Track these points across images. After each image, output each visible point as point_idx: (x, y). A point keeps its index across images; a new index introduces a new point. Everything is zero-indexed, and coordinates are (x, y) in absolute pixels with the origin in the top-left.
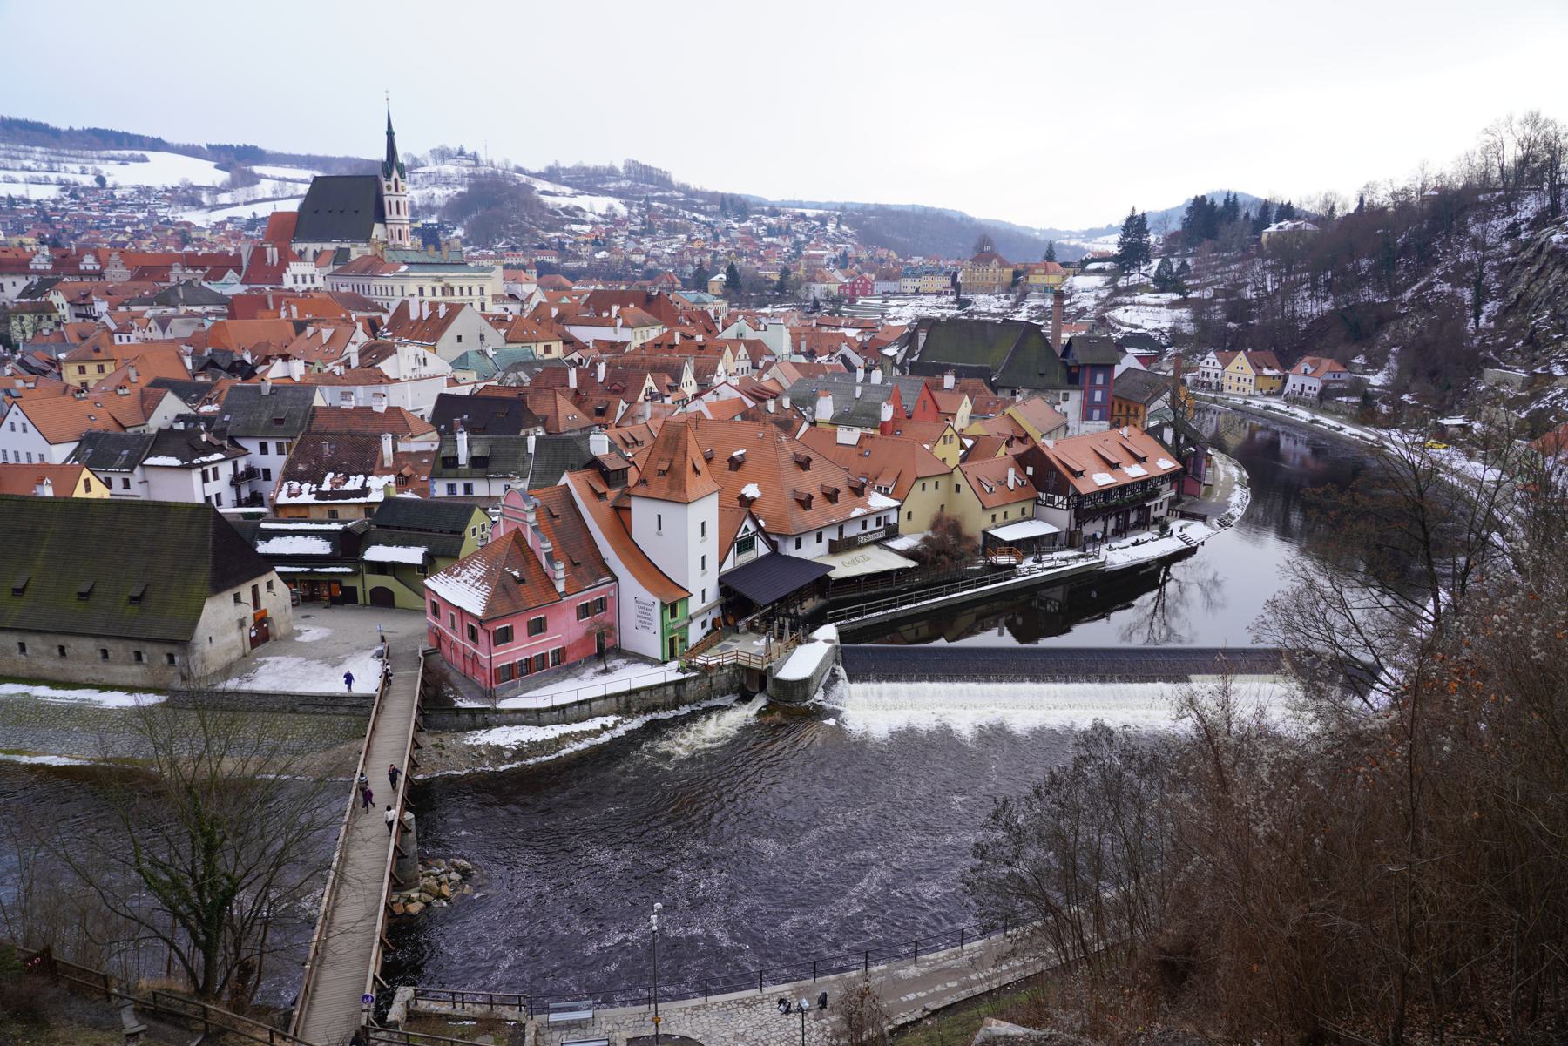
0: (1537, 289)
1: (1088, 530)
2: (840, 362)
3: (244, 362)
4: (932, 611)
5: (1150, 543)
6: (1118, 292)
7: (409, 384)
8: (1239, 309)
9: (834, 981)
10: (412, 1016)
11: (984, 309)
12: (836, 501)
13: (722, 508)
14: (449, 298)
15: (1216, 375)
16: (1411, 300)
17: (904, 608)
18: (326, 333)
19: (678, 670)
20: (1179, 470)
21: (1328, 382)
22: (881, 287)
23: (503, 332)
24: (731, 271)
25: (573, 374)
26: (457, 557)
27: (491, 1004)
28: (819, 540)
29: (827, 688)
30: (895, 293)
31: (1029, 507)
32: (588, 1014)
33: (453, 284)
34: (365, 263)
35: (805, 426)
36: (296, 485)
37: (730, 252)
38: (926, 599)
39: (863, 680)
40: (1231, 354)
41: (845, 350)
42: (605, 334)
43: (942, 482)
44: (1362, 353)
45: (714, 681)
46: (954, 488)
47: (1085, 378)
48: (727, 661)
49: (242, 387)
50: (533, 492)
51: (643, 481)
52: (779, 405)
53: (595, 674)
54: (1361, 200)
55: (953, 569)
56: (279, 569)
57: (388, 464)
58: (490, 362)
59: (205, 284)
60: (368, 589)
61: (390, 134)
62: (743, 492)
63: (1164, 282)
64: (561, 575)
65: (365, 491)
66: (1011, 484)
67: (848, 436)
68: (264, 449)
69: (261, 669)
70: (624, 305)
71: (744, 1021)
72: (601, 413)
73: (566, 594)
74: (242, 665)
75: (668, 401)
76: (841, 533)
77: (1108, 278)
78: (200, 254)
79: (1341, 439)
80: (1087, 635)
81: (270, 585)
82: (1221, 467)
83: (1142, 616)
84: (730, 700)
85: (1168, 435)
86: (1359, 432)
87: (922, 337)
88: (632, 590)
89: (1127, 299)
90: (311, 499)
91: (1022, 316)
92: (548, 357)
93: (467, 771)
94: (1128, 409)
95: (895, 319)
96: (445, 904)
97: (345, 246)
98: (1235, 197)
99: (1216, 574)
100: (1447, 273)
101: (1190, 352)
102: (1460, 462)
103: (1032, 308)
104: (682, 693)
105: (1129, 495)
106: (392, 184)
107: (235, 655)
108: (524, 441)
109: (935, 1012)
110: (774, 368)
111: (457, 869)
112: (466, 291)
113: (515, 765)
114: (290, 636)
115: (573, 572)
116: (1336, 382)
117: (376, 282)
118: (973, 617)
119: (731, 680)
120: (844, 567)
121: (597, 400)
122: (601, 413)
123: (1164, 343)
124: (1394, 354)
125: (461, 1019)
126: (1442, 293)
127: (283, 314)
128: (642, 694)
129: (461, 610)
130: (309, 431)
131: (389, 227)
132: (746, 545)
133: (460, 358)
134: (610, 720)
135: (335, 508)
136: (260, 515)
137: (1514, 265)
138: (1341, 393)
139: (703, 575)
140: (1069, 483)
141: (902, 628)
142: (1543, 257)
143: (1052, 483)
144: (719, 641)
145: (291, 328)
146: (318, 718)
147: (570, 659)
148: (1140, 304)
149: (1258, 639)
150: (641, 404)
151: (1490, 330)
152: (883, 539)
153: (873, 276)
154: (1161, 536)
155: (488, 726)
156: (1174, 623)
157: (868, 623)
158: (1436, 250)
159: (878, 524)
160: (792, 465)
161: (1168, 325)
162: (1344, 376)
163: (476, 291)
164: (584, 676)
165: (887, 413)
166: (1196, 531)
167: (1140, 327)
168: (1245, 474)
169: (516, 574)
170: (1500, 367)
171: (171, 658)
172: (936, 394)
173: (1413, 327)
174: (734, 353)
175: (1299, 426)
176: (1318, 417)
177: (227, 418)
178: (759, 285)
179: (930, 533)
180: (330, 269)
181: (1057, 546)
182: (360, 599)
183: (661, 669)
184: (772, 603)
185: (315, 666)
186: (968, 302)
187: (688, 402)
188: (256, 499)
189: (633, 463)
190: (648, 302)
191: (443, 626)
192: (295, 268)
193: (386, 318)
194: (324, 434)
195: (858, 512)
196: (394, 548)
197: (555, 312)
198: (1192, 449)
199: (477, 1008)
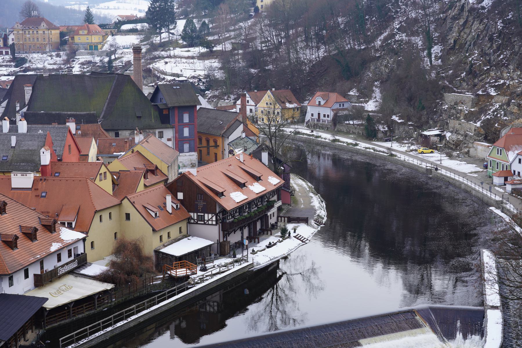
0: (465, 36)
1: (234, 238)
4: (140, 324)
5: (278, 244)
6: (154, 47)
11: (40, 66)
12: (36, 239)
15: (251, 110)
16: (382, 46)
17: (119, 324)
28: (27, 276)
31: (184, 225)
38: (133, 314)
40: (259, 94)
44: (355, 87)
46: (124, 216)
47: (174, 117)
66: (169, 209)
76: (42, 268)
77: (142, 36)
85: (265, 156)
91: (76, 70)
94: (208, 141)
101: (225, 94)
102: (447, 162)
103: (83, 64)
123: (202, 88)
124: (376, 87)
126: (402, 41)
137: (445, 19)
138: (347, 118)
140: (216, 202)
142: (465, 14)
143: (201, 204)
148: (175, 57)
151: (440, 66)
156: (288, 307)
157: (94, 343)
159: (70, 256)
161: (202, 73)
162: (346, 105)
165: (46, 158)
167: (182, 76)
168: (309, 184)
170: (455, 92)
173: (386, 66)
175: (324, 145)
176: (337, 138)
179: (114, 258)
181: (213, 256)
186: (23, 61)
195: (55, 247)
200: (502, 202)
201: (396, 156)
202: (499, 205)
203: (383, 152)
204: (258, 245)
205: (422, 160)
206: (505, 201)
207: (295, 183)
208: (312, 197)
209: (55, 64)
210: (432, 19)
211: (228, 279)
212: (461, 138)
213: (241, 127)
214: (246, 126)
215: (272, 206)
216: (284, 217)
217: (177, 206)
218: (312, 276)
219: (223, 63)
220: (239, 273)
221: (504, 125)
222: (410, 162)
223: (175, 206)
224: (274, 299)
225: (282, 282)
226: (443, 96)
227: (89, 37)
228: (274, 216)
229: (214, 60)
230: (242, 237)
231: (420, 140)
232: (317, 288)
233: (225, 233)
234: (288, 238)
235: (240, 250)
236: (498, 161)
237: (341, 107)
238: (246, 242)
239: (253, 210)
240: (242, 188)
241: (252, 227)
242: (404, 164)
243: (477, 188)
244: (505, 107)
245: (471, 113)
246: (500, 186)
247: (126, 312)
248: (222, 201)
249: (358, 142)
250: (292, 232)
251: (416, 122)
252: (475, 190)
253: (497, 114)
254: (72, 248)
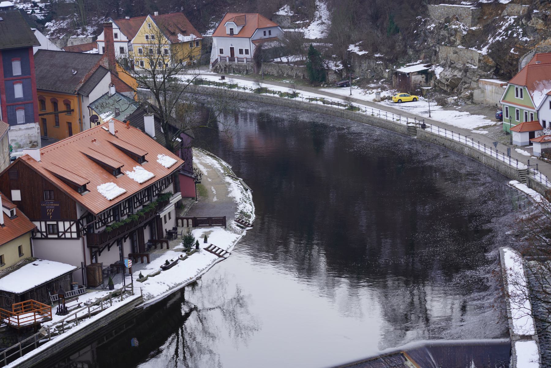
5: (181, 262)
15: (122, 49)
21: (262, 41)
31: (25, 243)
79: (299, 107)
85: (149, 122)
86: (318, 96)
94: (55, 104)
99: (239, 291)
116: (271, 40)
123: (40, 17)
138: (277, 52)
143: (51, 206)
162: (275, 33)
168: (224, 163)
175: (244, 98)
176: (264, 85)
181: (76, 289)
200: (528, 172)
201: (359, 109)
202: (523, 176)
203: (338, 104)
204: (148, 266)
205: (400, 113)
206: (532, 170)
207: (201, 163)
208: (229, 184)
211: (103, 324)
212: (458, 74)
213: (108, 78)
214: (115, 75)
215: (167, 203)
216: (187, 219)
217: (12, 212)
218: (238, 310)
220: (120, 314)
221: (523, 50)
222: (382, 117)
223: (8, 213)
224: (180, 351)
225: (191, 323)
226: (427, 9)
228: (170, 218)
230: (122, 256)
231: (395, 81)
232: (246, 328)
233: (94, 250)
234: (195, 251)
235: (119, 276)
236: (518, 107)
237: (267, 36)
238: (128, 263)
239: (135, 211)
240: (115, 176)
241: (136, 237)
242: (373, 122)
243: (488, 152)
244: (524, 21)
245: (471, 34)
246: (523, 147)
248: (85, 199)
249: (297, 91)
250: (201, 241)
251: (386, 54)
252: (484, 155)
253: (512, 34)
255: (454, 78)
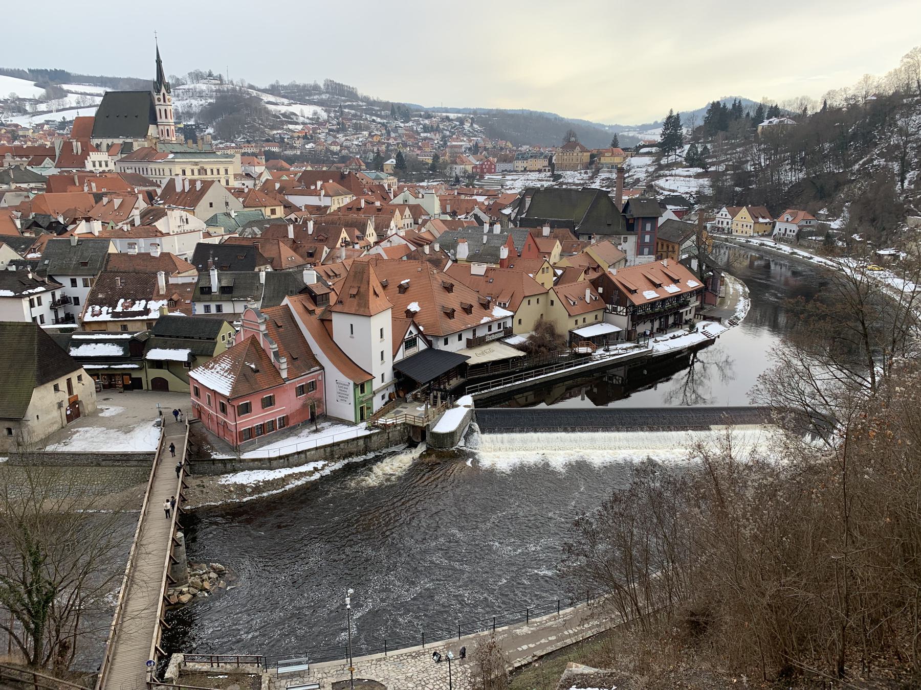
1: (641, 328)
2: (473, 219)
3: (59, 222)
4: (536, 385)
6: (661, 167)
7: (176, 236)
8: (742, 178)
9: (472, 639)
10: (182, 674)
11: (570, 181)
13: (394, 319)
14: (203, 177)
16: (858, 170)
17: (517, 383)
18: (117, 202)
19: (366, 429)
20: (702, 288)
22: (501, 167)
23: (241, 200)
24: (399, 157)
25: (291, 228)
26: (212, 356)
27: (238, 663)
28: (460, 339)
29: (466, 438)
30: (510, 171)
31: (600, 314)
32: (305, 667)
33: (206, 166)
34: (145, 152)
35: (450, 263)
36: (97, 308)
37: (398, 144)
38: (532, 377)
39: (490, 432)
40: (737, 209)
41: (477, 210)
42: (313, 201)
43: (541, 298)
44: (826, 207)
45: (390, 435)
48: (399, 422)
49: (57, 240)
50: (263, 310)
51: (340, 302)
52: (432, 249)
53: (309, 433)
54: (825, 103)
55: (549, 357)
56: (86, 367)
57: (162, 292)
58: (233, 220)
59: (29, 168)
60: (150, 378)
61: (159, 62)
62: (409, 308)
63: (692, 161)
64: (284, 366)
65: (146, 311)
66: (588, 300)
67: (478, 269)
68: (74, 283)
69: (75, 437)
70: (325, 180)
71: (412, 668)
72: (311, 255)
73: (288, 379)
74: (62, 434)
75: (357, 247)
76: (474, 334)
78: (25, 146)
79: (811, 265)
80: (641, 399)
81: (80, 378)
82: (731, 285)
83: (678, 386)
84: (402, 446)
85: (694, 264)
86: (824, 260)
87: (528, 201)
88: (334, 375)
89: (667, 172)
90: (105, 317)
91: (596, 185)
92: (273, 217)
93: (221, 502)
94: (668, 247)
95: (510, 189)
96: (206, 595)
97: (129, 140)
98: (740, 102)
100: (882, 152)
101: (710, 208)
103: (603, 180)
104: (369, 444)
105: (668, 305)
106: (161, 97)
107: (55, 427)
108: (257, 275)
109: (541, 657)
110: (429, 223)
111: (214, 570)
112: (215, 172)
113: (254, 497)
114: (96, 413)
115: (293, 364)
117: (152, 166)
118: (564, 388)
119: (402, 434)
120: (477, 357)
121: (308, 247)
122: (311, 255)
123: (692, 202)
124: (847, 207)
125: (217, 674)
126: (879, 165)
127: (86, 189)
128: (342, 446)
129: (215, 392)
130: (106, 270)
131: (161, 127)
132: (411, 343)
133: (212, 218)
134: (320, 464)
135: (125, 323)
136: (72, 329)
138: (811, 234)
139: (382, 363)
140: (627, 297)
141: (516, 397)
143: (615, 298)
144: (394, 408)
145: (93, 201)
146: (116, 469)
147: (292, 423)
148: (676, 175)
149: (754, 401)
150: (339, 249)
151: (911, 190)
152: (502, 338)
153: (496, 160)
154: (690, 332)
155: (235, 471)
156: (700, 391)
157: (493, 394)
158: (875, 137)
159: (499, 327)
160: (441, 288)
161: (695, 190)
162: (813, 223)
163: (222, 172)
164: (301, 434)
165: (504, 253)
166: (714, 328)
167: (676, 191)
168: (747, 289)
169: (253, 366)
171: (10, 431)
172: (537, 240)
173: (860, 189)
174: (402, 213)
175: (784, 257)
176: (796, 251)
177: (46, 262)
178: (418, 166)
179: (534, 333)
180: (119, 157)
181: (620, 340)
182: (145, 386)
183: (354, 428)
184: (429, 382)
185: (113, 433)
186: (560, 176)
187: (371, 248)
188: (69, 318)
189: (333, 290)
190: (342, 179)
191: (203, 403)
192: (94, 156)
193: (159, 191)
194: (117, 273)
195: (485, 320)
196: (167, 350)
197: (277, 186)
198: (711, 273)
199: (228, 666)
209: (582, 179)
210: (914, 145)
219: (713, 182)
223: (594, 298)
227: (612, 158)
229: (707, 179)
235: (643, 339)
247: (525, 374)
249: (813, 256)
254: (502, 322)
255: (910, 260)
